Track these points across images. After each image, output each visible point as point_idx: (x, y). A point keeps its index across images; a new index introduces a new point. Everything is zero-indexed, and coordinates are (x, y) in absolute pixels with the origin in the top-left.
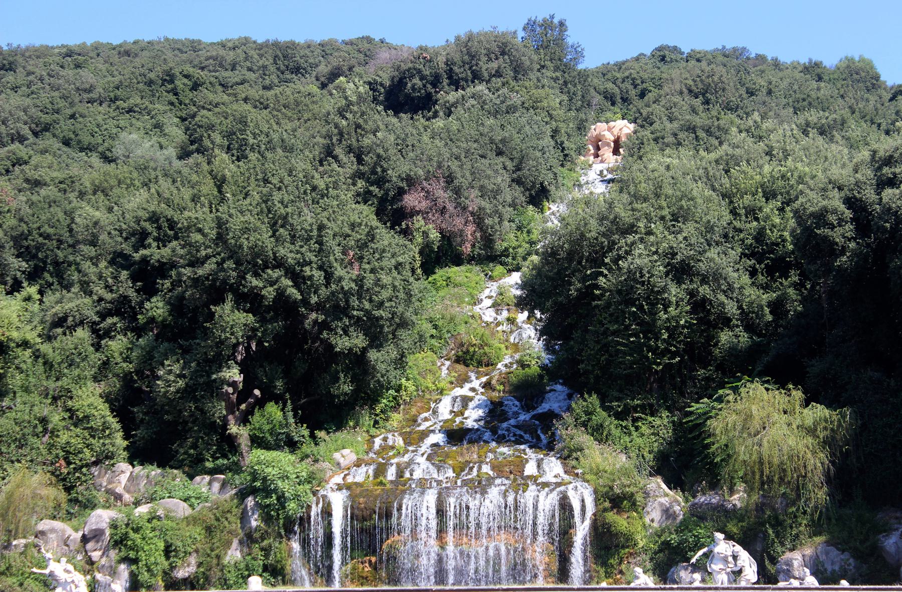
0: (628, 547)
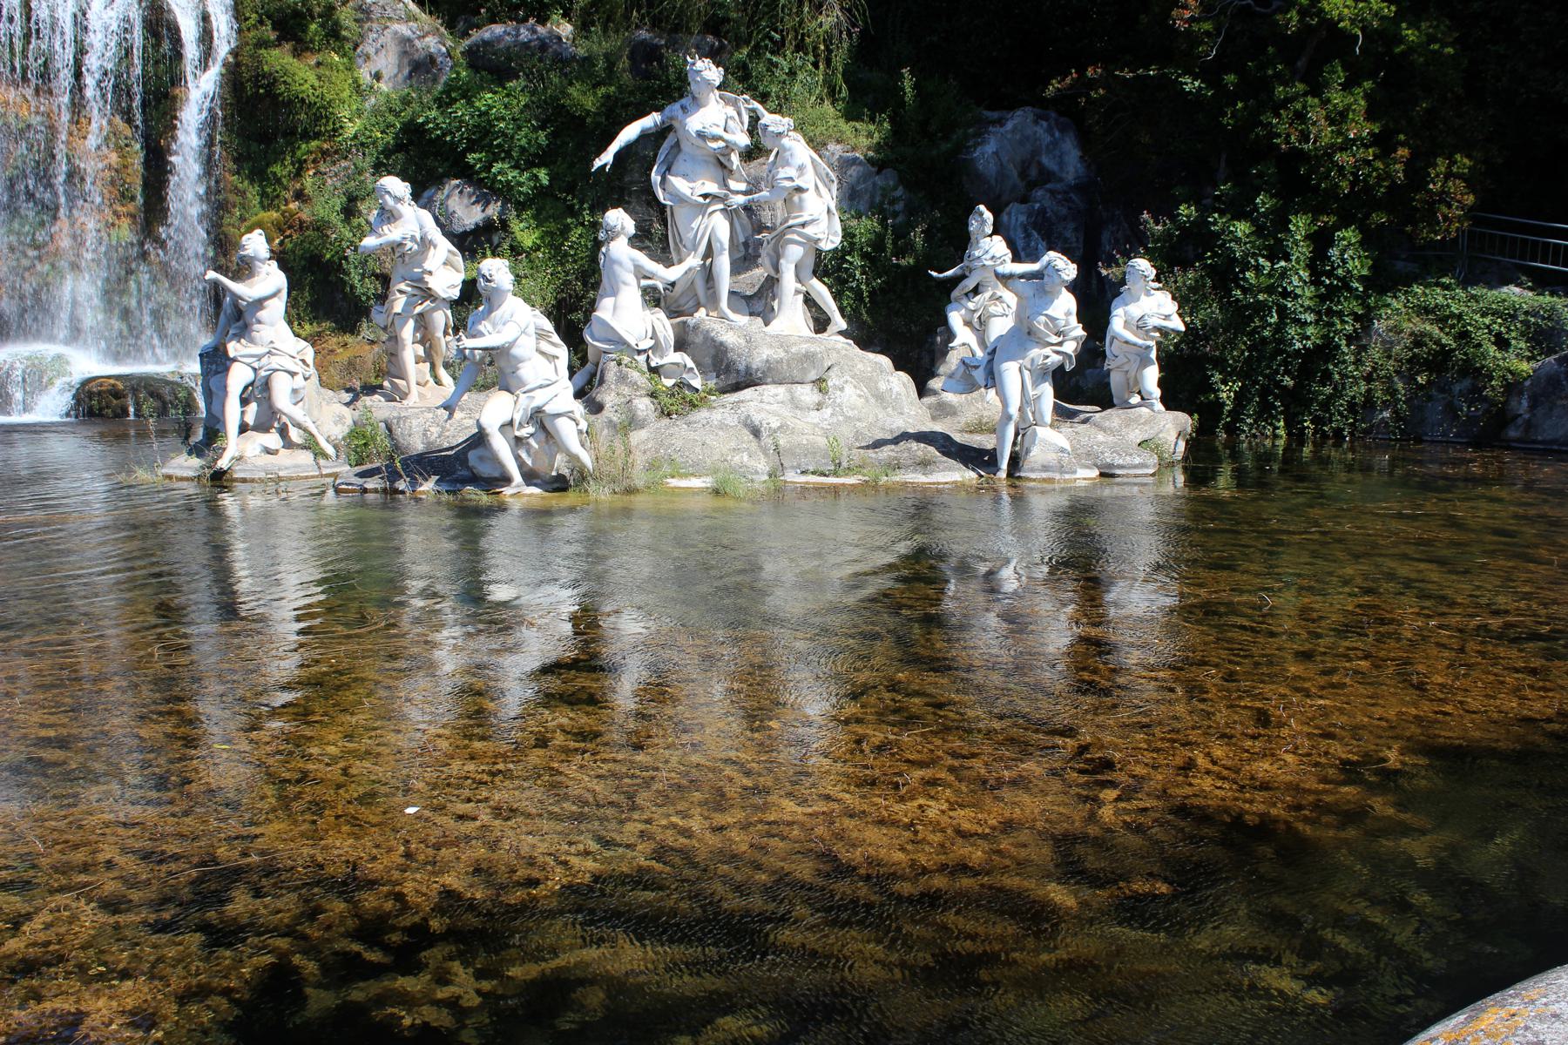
0: (317, 136)
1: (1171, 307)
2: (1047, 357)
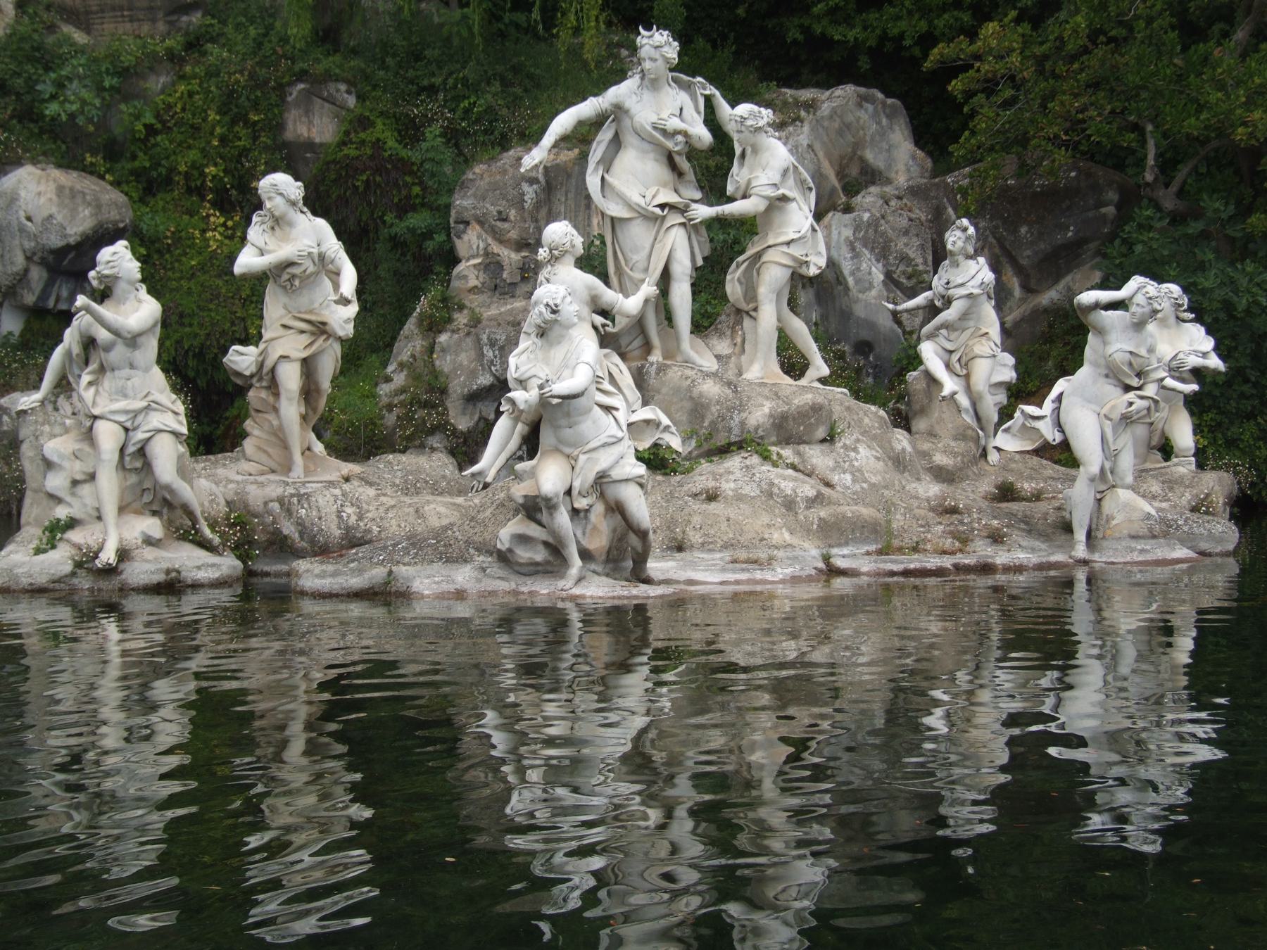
1: (1208, 344)
2: (1131, 404)
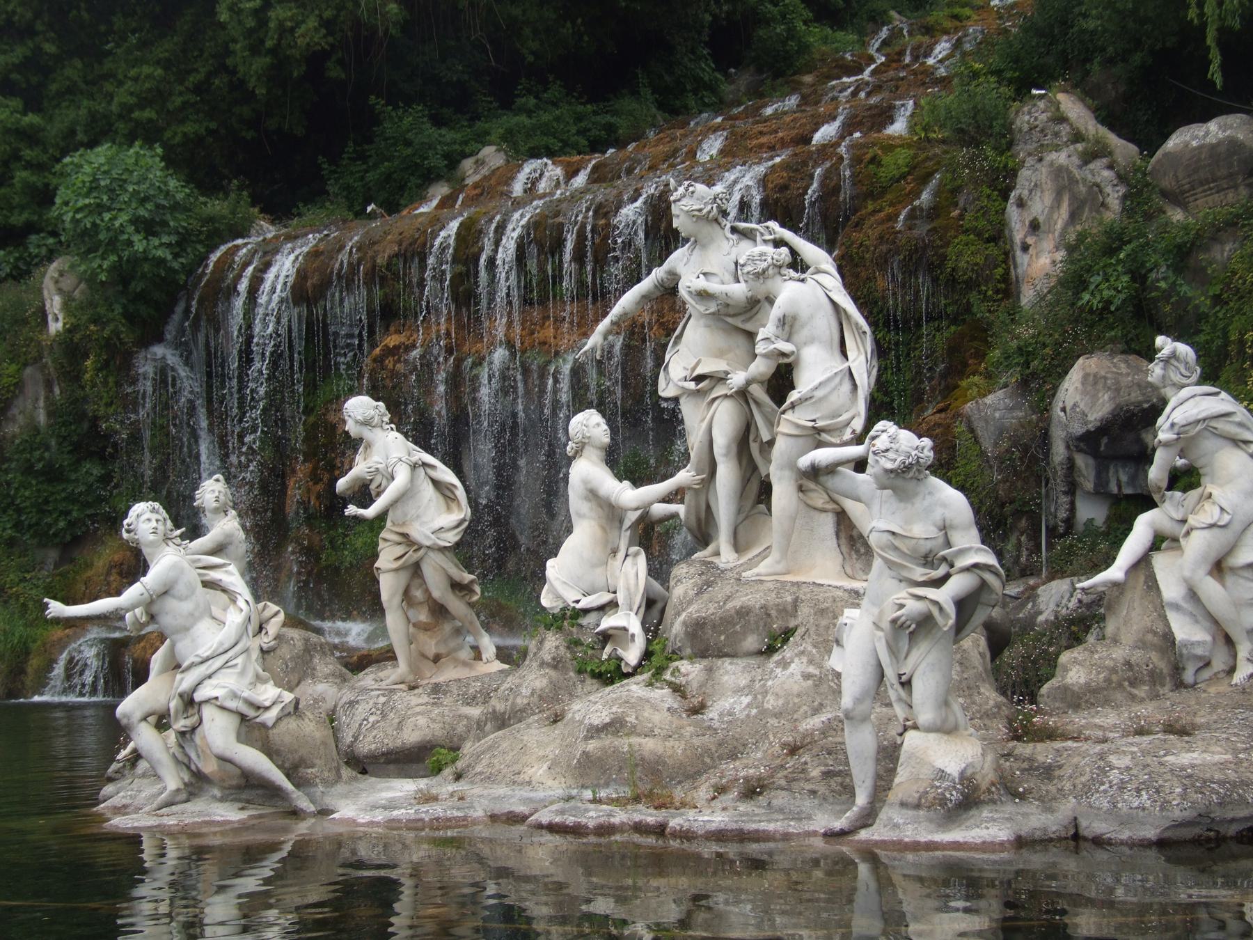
2: (902, 606)
